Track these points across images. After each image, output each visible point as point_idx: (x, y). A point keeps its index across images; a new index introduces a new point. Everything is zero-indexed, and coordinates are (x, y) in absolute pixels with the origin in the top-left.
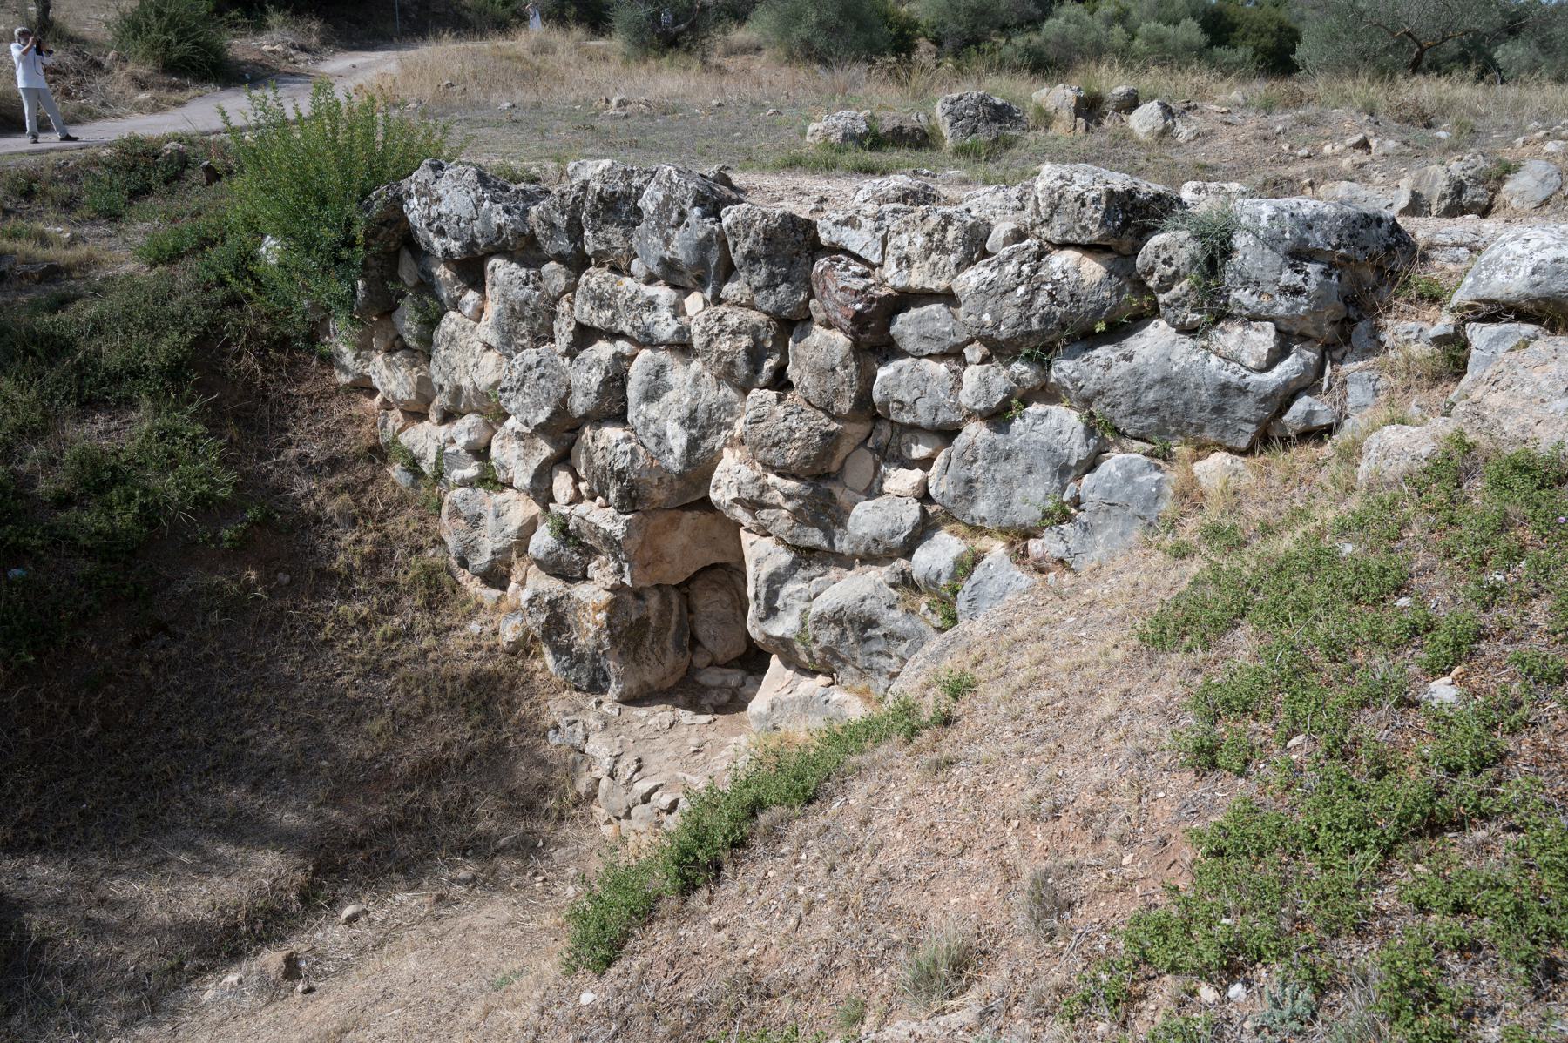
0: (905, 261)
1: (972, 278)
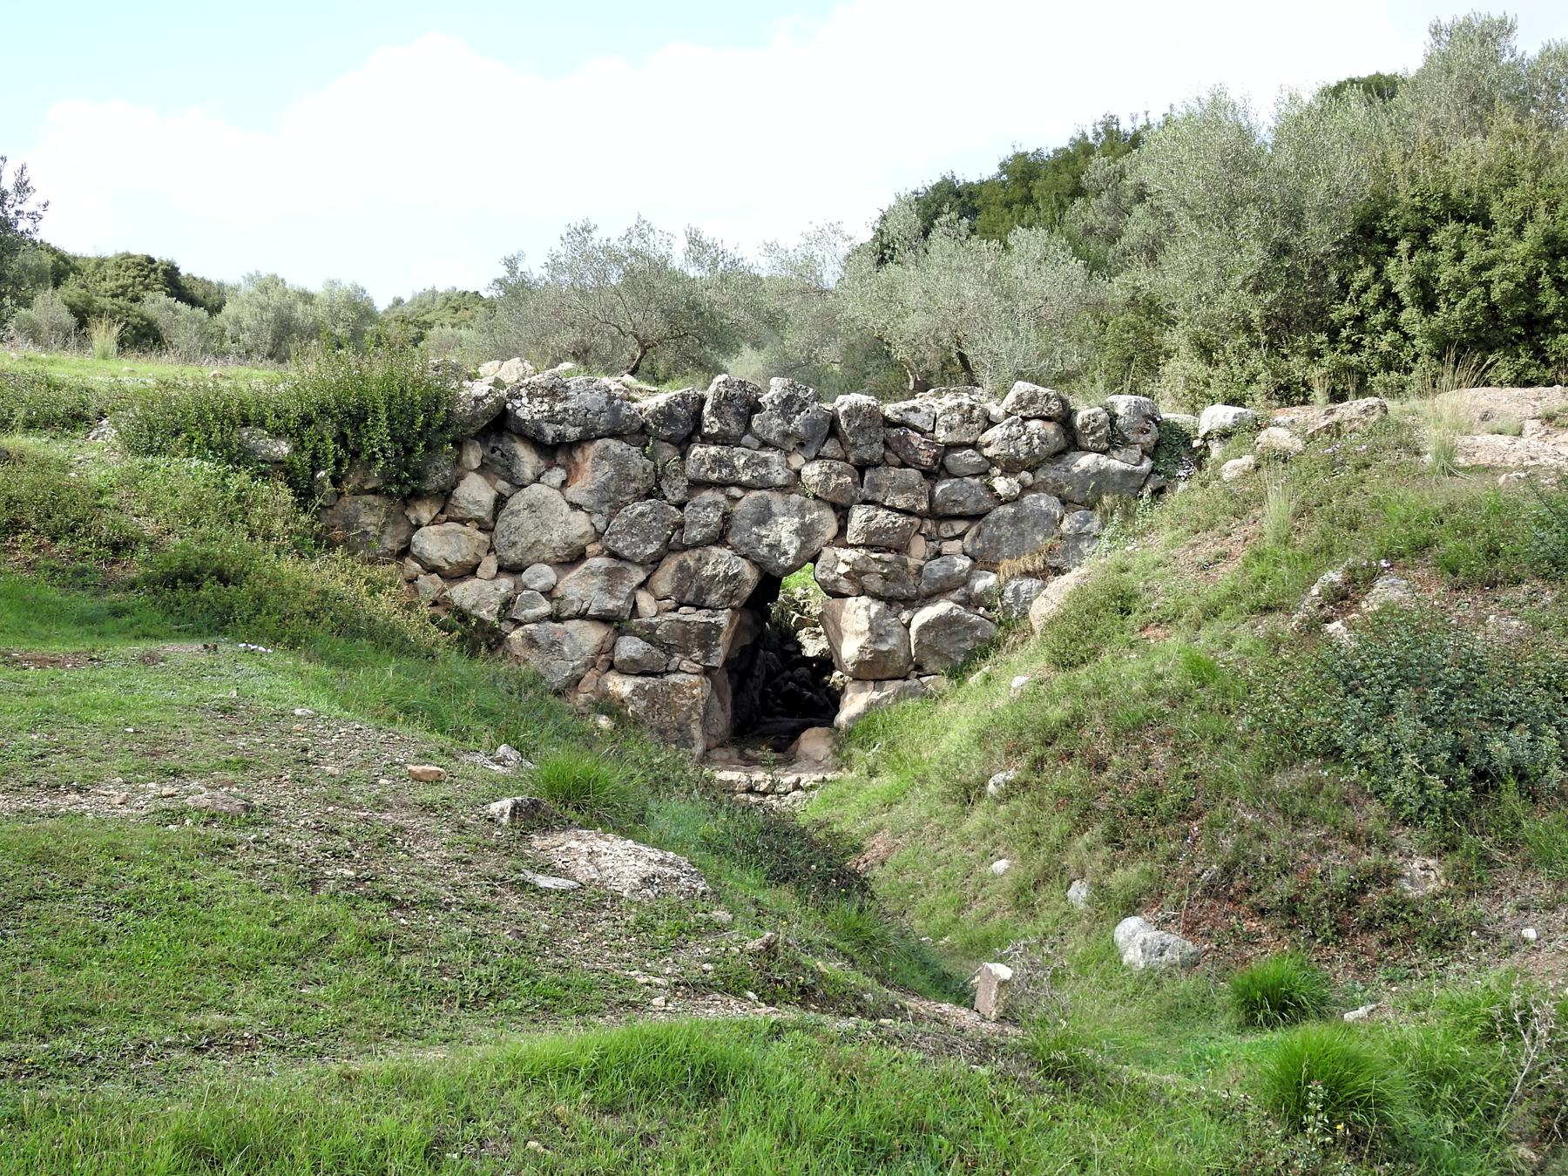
0: (950, 428)
1: (994, 433)
